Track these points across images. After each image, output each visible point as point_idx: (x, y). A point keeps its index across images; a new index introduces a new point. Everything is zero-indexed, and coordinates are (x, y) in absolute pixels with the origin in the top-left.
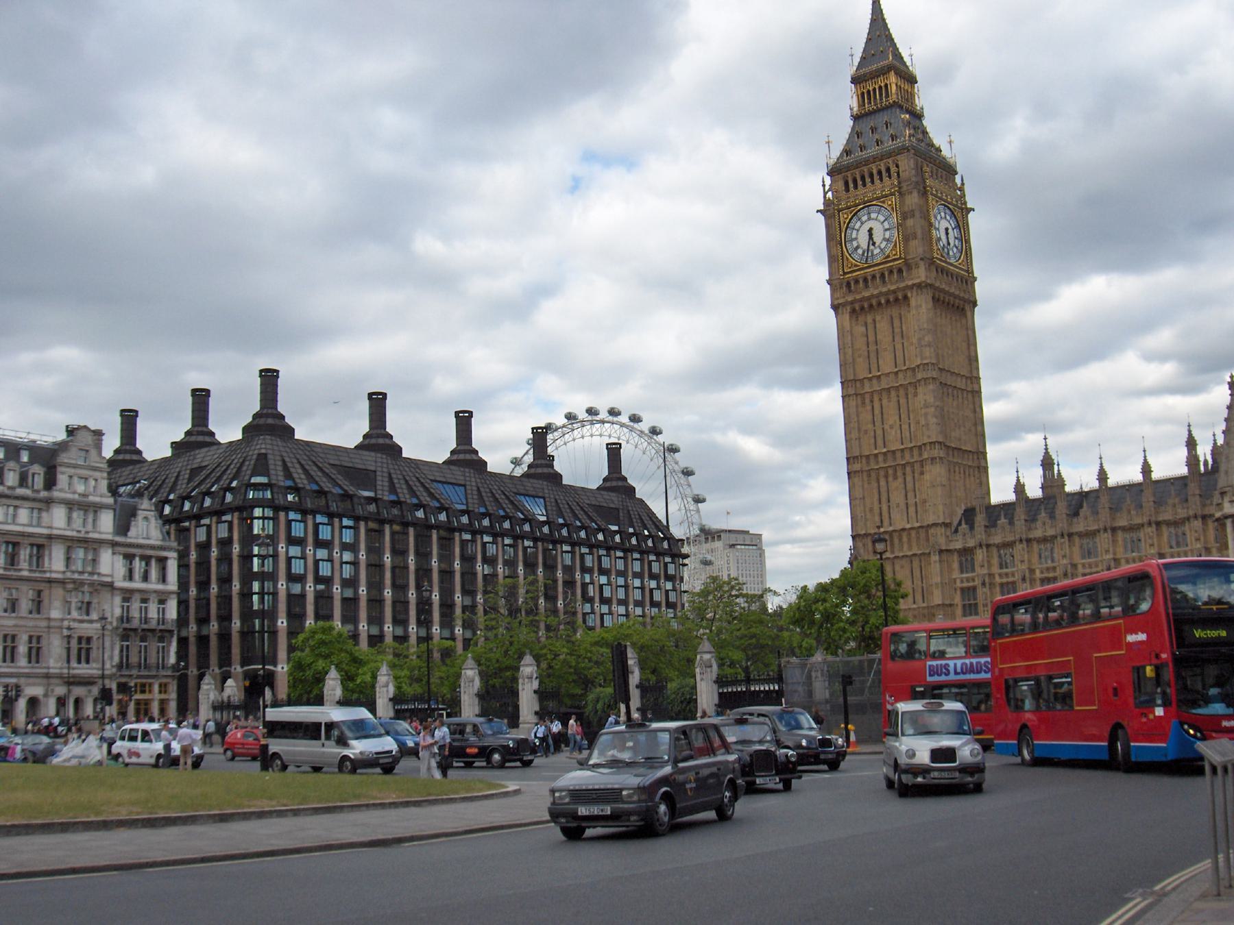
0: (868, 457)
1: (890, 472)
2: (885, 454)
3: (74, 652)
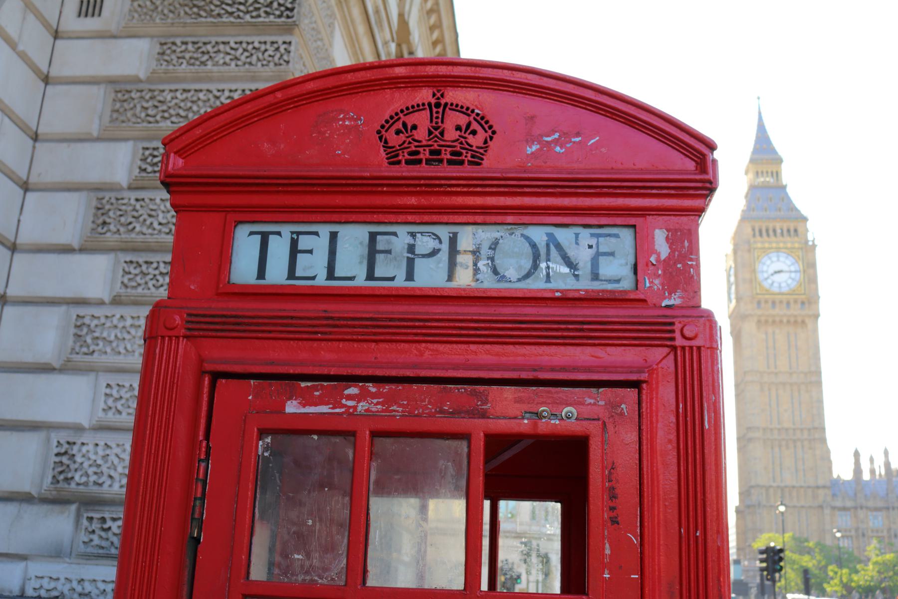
0: (764, 429)
1: (784, 443)
2: (779, 430)
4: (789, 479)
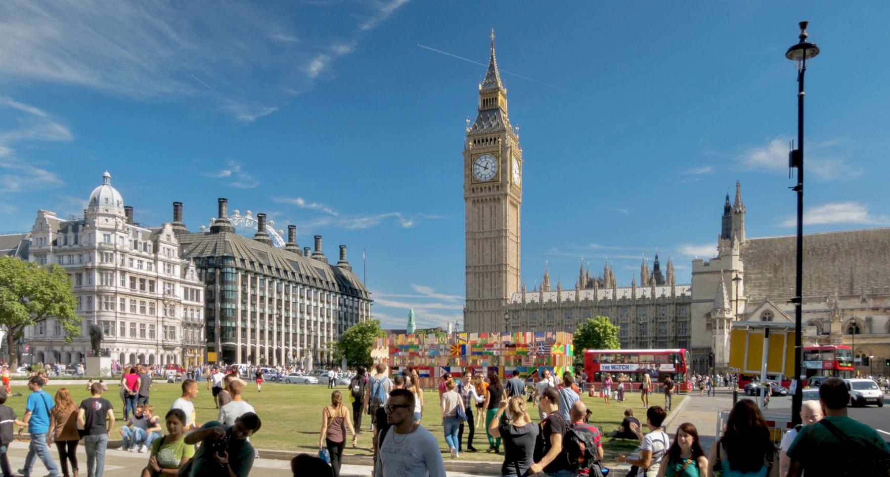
3: (168, 333)
4: (487, 295)
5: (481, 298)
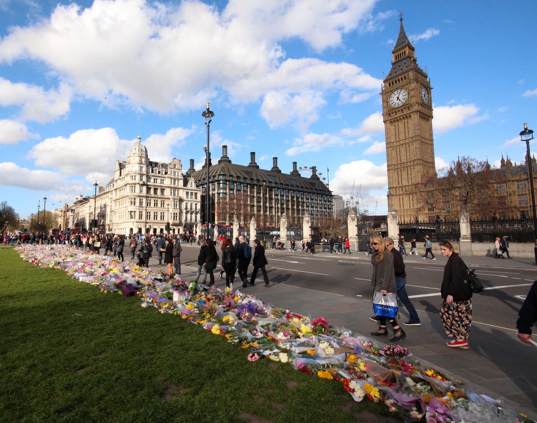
1: (402, 169)
5: (400, 185)
